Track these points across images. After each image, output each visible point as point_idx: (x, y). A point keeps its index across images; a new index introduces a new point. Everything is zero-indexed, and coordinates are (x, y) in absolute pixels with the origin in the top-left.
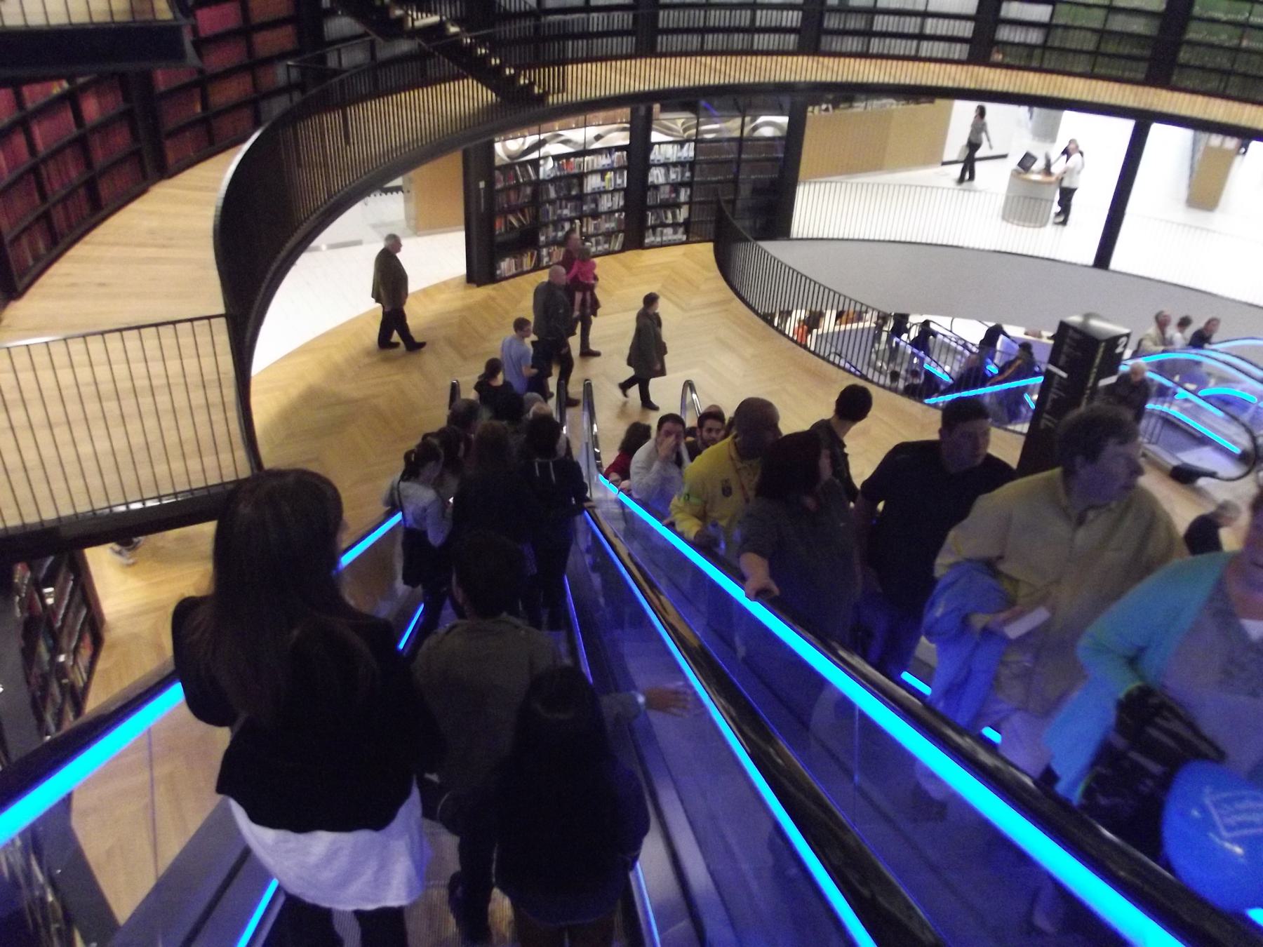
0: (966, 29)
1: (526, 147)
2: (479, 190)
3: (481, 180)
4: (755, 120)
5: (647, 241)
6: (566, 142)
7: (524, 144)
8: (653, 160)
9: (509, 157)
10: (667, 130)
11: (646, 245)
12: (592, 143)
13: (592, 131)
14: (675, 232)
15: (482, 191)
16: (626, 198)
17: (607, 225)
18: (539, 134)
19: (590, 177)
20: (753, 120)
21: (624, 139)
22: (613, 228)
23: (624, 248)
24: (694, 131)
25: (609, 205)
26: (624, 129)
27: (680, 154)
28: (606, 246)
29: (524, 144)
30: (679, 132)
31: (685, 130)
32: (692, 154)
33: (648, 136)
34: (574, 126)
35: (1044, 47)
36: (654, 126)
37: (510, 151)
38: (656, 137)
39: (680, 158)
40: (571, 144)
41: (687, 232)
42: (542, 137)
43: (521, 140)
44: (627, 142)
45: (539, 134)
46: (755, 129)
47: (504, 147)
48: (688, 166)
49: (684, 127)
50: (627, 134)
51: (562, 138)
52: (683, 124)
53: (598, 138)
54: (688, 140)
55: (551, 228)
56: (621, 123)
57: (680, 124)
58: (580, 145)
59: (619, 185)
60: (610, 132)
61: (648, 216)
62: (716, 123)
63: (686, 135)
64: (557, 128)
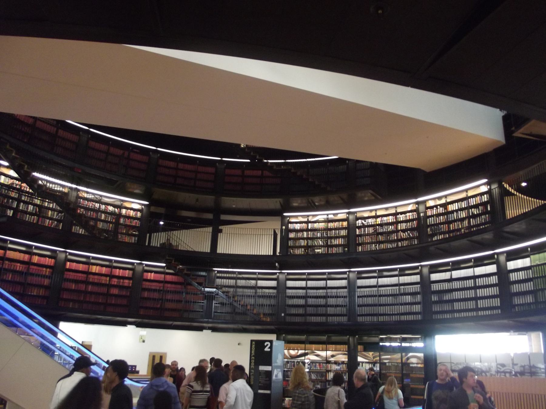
0: (497, 302)
6: (318, 356)
7: (298, 353)
9: (290, 356)
10: (365, 357)
12: (330, 358)
13: (329, 353)
18: (305, 350)
20: (406, 355)
21: (345, 358)
24: (378, 358)
29: (298, 353)
30: (371, 358)
31: (374, 358)
34: (321, 349)
35: (536, 302)
37: (292, 354)
40: (320, 357)
42: (306, 351)
43: (296, 351)
45: (305, 350)
46: (408, 359)
49: (373, 356)
50: (346, 356)
51: (316, 354)
52: (372, 355)
53: (333, 356)
56: (343, 351)
57: (371, 355)
58: (324, 358)
60: (338, 354)
62: (388, 355)
63: (374, 360)
64: (313, 349)
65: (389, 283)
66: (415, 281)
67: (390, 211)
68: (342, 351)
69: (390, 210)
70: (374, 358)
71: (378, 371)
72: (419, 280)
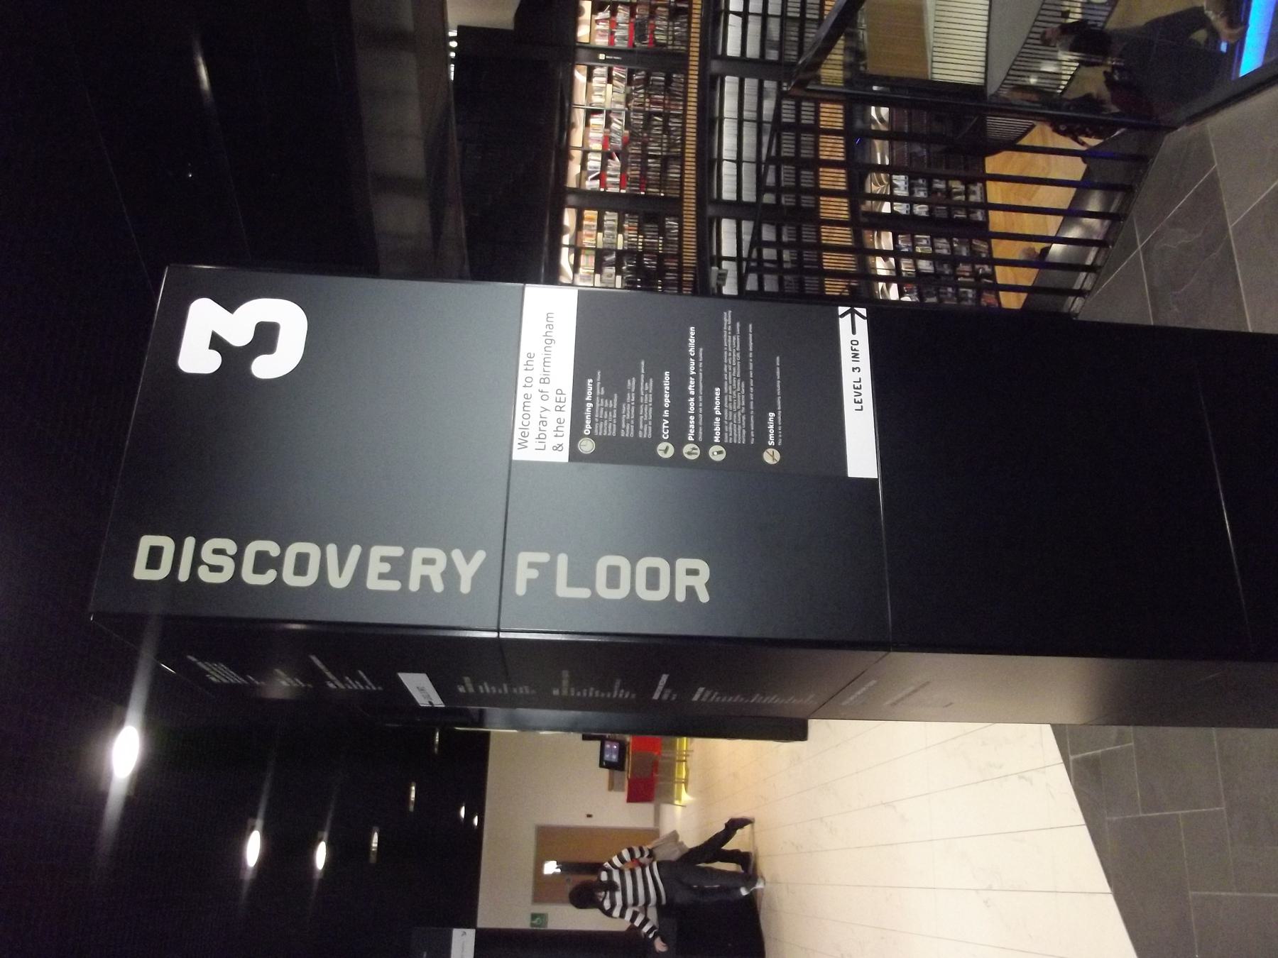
4: (875, 121)
8: (907, 212)
12: (890, 264)
14: (974, 193)
16: (940, 236)
19: (920, 267)
20: (873, 121)
21: (888, 236)
22: (967, 249)
26: (879, 236)
27: (902, 188)
31: (881, 183)
32: (903, 177)
33: (886, 215)
36: (877, 210)
39: (906, 188)
41: (974, 182)
44: (890, 234)
46: (882, 120)
48: (912, 181)
50: (883, 234)
52: (876, 185)
54: (890, 180)
56: (873, 237)
59: (928, 242)
61: (957, 217)
62: (876, 156)
65: (735, 141)
66: (736, 88)
67: (578, 118)
68: (874, 240)
69: (576, 118)
70: (881, 183)
71: (906, 178)
72: (736, 79)
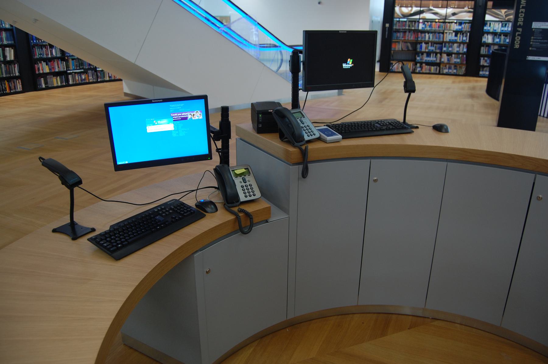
1: (412, 12)
2: (386, 27)
3: (388, 23)
5: (481, 73)
6: (435, 14)
7: (411, 10)
8: (485, 30)
11: (480, 75)
12: (450, 16)
13: (450, 11)
15: (387, 28)
16: (468, 48)
17: (456, 60)
21: (469, 17)
22: (458, 62)
23: (465, 75)
25: (458, 49)
26: (469, 12)
27: (503, 29)
28: (455, 71)
29: (411, 10)
30: (503, 16)
31: (506, 16)
34: (440, 6)
36: (487, 12)
37: (403, 12)
38: (488, 17)
39: (503, 31)
40: (438, 15)
42: (422, 9)
43: (410, 9)
44: (471, 19)
47: (400, 10)
50: (471, 14)
51: (433, 11)
52: (505, 12)
53: (454, 14)
54: (509, 21)
55: (425, 55)
58: (444, 16)
59: (464, 40)
61: (481, 59)
63: (506, 19)
